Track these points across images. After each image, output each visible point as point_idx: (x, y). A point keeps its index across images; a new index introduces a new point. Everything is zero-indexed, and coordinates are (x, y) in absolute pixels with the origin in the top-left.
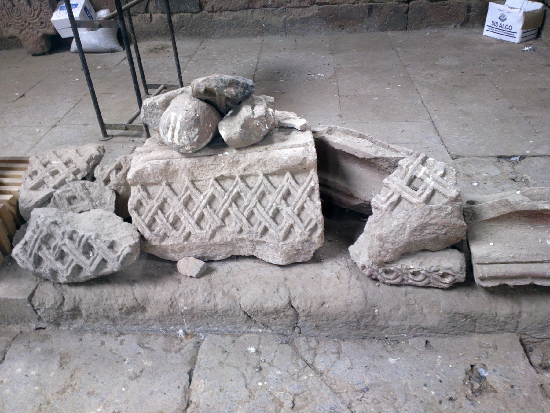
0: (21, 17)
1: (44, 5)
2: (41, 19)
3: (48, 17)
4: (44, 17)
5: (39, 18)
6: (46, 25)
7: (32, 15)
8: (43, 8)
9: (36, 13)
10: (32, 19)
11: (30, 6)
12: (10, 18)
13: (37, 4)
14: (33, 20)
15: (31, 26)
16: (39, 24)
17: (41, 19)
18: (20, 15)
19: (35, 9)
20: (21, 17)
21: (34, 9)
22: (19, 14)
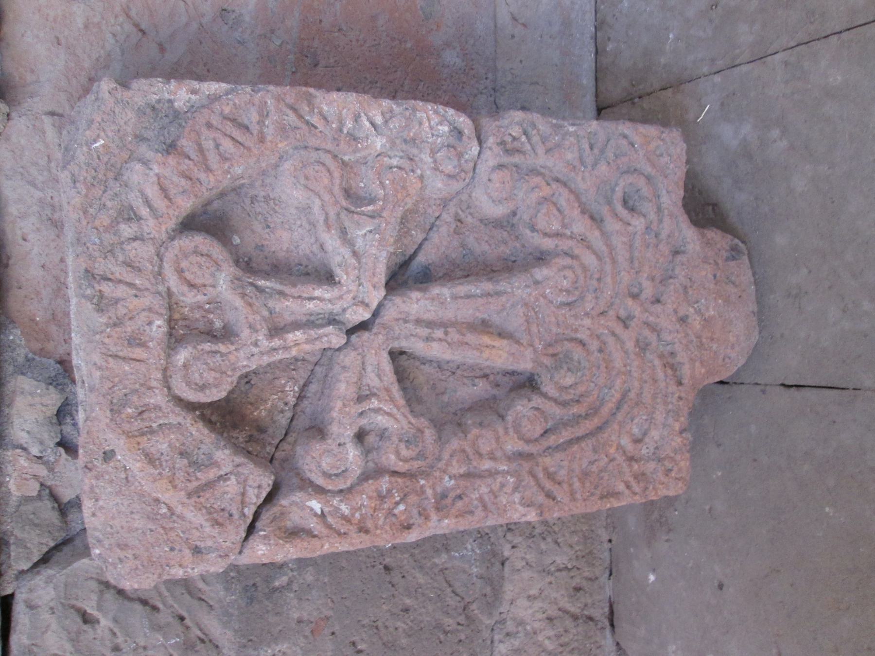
0: (594, 345)
1: (541, 150)
2: (609, 202)
3: (602, 151)
4: (603, 168)
5: (605, 210)
6: (648, 178)
7: (589, 259)
8: (554, 164)
9: (580, 226)
10: (608, 268)
11: (541, 258)
12: (600, 429)
13: (534, 197)
14: (614, 261)
15: (648, 290)
16: (638, 223)
17: (609, 202)
18: (582, 343)
19: (556, 226)
20: (594, 345)
21: (557, 235)
22: (577, 353)
